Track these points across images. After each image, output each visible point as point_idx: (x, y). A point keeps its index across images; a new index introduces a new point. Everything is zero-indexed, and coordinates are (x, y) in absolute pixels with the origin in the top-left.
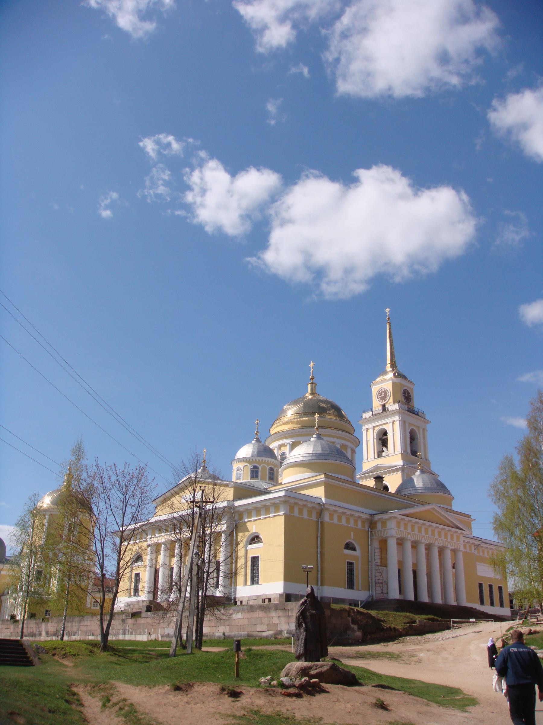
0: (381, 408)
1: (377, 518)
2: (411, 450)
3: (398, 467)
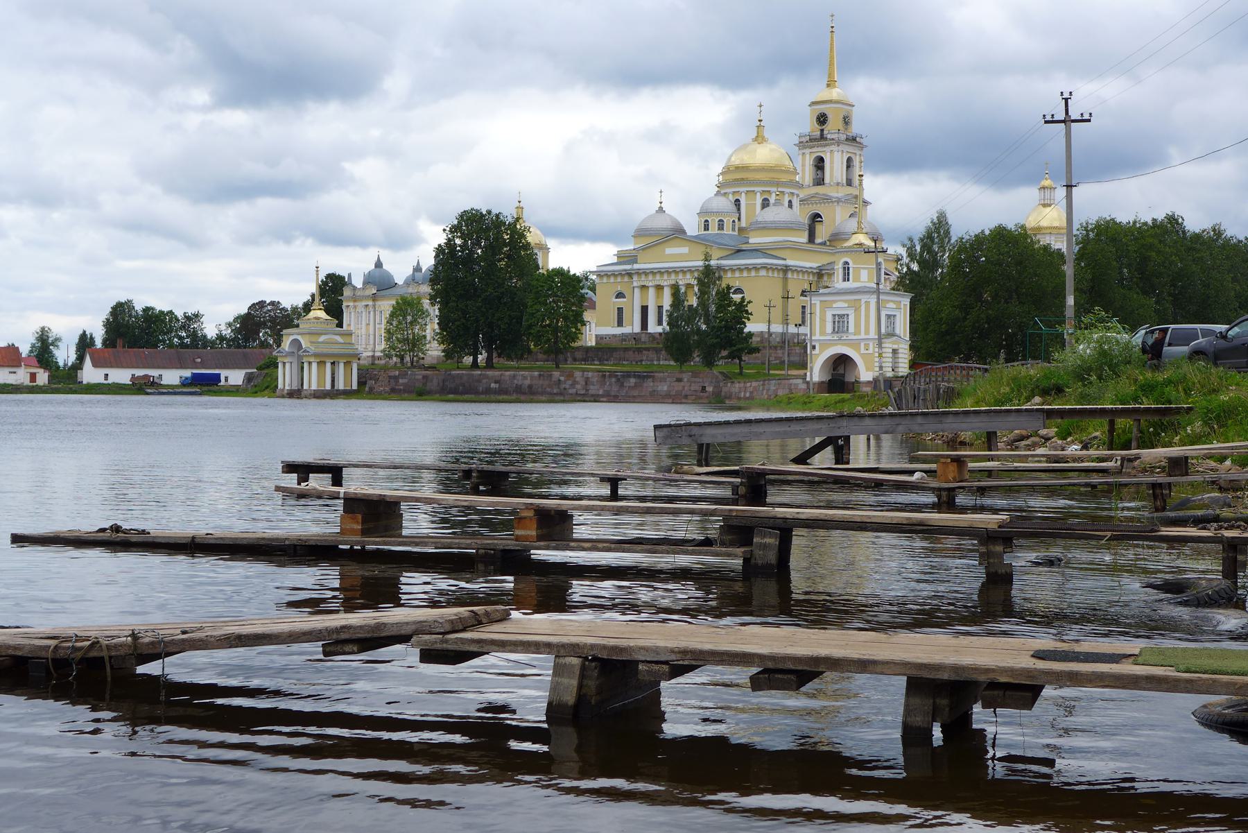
0: (819, 133)
1: (824, 272)
2: (847, 179)
3: (834, 200)
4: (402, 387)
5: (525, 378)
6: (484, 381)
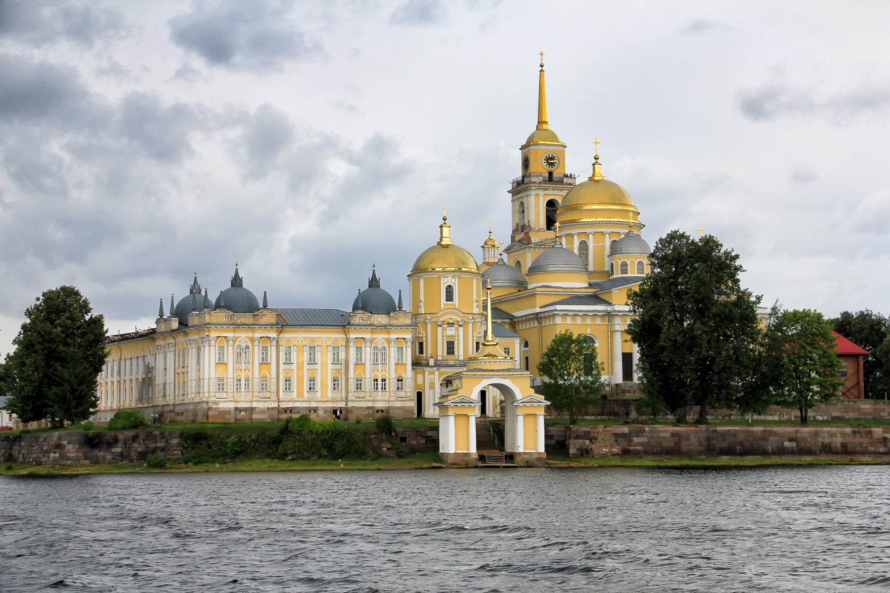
4: (640, 448)
5: (832, 435)
6: (772, 439)
